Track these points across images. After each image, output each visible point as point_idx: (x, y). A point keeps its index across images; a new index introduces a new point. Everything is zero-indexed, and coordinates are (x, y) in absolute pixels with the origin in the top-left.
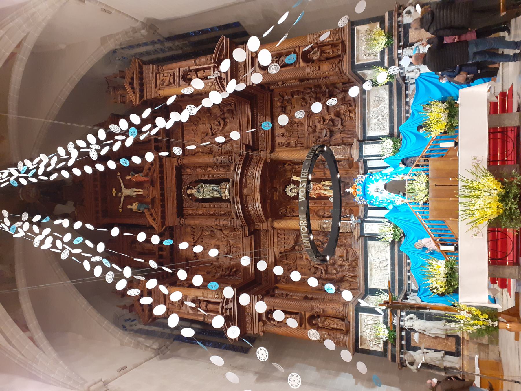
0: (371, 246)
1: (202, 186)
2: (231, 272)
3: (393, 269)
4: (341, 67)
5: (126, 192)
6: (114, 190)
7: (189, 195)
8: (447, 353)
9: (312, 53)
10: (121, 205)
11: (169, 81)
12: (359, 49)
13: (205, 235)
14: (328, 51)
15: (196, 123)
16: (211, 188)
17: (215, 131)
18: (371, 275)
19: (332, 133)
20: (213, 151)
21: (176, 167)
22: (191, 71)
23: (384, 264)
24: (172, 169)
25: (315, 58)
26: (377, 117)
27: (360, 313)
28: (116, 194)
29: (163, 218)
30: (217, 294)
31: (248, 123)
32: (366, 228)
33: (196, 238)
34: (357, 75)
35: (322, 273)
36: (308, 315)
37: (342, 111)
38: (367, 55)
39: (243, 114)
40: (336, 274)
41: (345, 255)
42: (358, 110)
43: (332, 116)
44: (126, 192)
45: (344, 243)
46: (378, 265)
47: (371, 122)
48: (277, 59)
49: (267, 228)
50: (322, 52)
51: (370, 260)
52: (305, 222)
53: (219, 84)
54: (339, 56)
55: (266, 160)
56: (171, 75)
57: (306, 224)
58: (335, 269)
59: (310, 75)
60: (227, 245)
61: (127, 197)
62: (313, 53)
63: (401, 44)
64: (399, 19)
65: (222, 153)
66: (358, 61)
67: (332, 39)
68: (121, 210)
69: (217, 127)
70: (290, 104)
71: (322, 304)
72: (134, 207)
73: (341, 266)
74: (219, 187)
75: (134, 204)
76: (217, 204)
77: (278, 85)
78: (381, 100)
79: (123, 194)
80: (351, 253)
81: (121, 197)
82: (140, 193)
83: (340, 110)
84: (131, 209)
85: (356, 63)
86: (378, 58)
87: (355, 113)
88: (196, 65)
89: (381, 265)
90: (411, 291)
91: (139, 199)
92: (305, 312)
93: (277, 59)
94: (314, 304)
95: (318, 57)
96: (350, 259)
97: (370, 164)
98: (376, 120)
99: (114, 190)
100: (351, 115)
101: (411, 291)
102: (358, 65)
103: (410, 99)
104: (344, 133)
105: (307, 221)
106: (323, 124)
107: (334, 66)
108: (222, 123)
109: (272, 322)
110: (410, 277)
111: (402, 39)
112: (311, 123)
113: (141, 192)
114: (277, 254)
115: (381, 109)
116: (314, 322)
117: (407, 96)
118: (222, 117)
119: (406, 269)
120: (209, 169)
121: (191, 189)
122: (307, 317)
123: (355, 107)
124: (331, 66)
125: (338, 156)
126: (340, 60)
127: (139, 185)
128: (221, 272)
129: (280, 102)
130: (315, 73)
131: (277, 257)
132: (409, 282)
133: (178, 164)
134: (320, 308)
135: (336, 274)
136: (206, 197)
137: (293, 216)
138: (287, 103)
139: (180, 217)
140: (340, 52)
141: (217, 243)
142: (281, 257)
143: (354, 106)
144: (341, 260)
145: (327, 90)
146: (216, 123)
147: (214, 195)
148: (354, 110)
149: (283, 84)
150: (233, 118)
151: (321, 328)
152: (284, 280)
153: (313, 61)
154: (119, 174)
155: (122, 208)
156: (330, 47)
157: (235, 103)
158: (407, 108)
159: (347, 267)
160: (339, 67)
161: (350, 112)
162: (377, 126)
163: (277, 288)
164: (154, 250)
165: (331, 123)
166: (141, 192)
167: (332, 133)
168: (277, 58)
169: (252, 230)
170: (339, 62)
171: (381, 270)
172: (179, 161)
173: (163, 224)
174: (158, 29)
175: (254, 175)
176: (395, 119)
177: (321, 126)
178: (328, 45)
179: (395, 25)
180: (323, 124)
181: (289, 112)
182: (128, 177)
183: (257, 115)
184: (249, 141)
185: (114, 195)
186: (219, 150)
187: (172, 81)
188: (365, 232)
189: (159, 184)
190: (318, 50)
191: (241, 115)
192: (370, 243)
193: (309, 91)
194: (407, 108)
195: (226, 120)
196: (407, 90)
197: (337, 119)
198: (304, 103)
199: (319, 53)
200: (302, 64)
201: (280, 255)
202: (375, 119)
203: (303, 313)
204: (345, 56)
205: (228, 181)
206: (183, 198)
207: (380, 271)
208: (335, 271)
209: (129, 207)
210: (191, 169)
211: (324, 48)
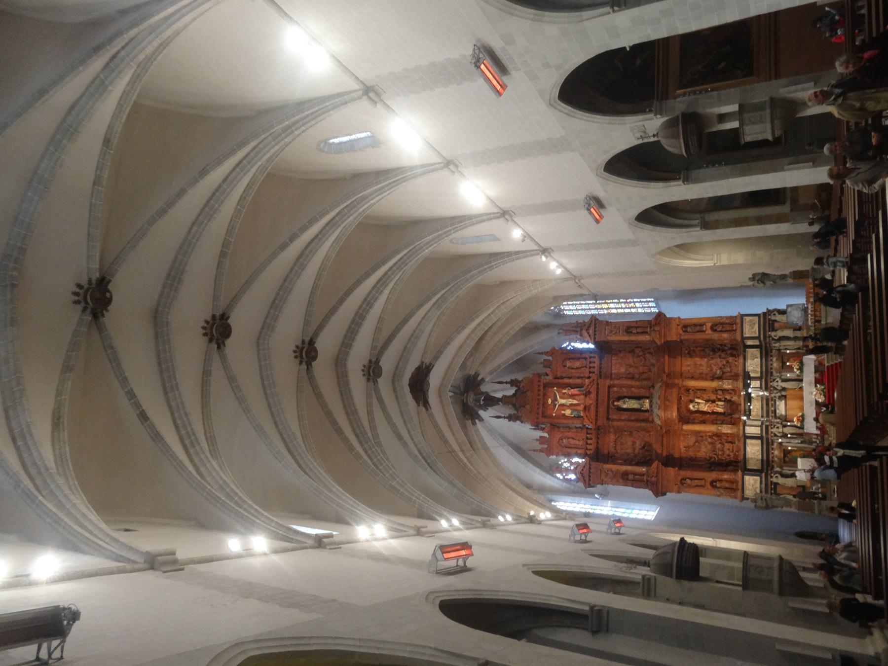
5: (563, 401)
7: (614, 405)
23: (758, 453)
25: (718, 330)
36: (710, 480)
44: (563, 401)
54: (734, 330)
61: (563, 405)
72: (568, 412)
76: (637, 413)
86: (757, 335)
100: (736, 363)
151: (719, 488)
158: (771, 363)
167: (724, 373)
179: (767, 320)
192: (748, 441)
194: (771, 363)
205: (648, 398)
209: (563, 412)
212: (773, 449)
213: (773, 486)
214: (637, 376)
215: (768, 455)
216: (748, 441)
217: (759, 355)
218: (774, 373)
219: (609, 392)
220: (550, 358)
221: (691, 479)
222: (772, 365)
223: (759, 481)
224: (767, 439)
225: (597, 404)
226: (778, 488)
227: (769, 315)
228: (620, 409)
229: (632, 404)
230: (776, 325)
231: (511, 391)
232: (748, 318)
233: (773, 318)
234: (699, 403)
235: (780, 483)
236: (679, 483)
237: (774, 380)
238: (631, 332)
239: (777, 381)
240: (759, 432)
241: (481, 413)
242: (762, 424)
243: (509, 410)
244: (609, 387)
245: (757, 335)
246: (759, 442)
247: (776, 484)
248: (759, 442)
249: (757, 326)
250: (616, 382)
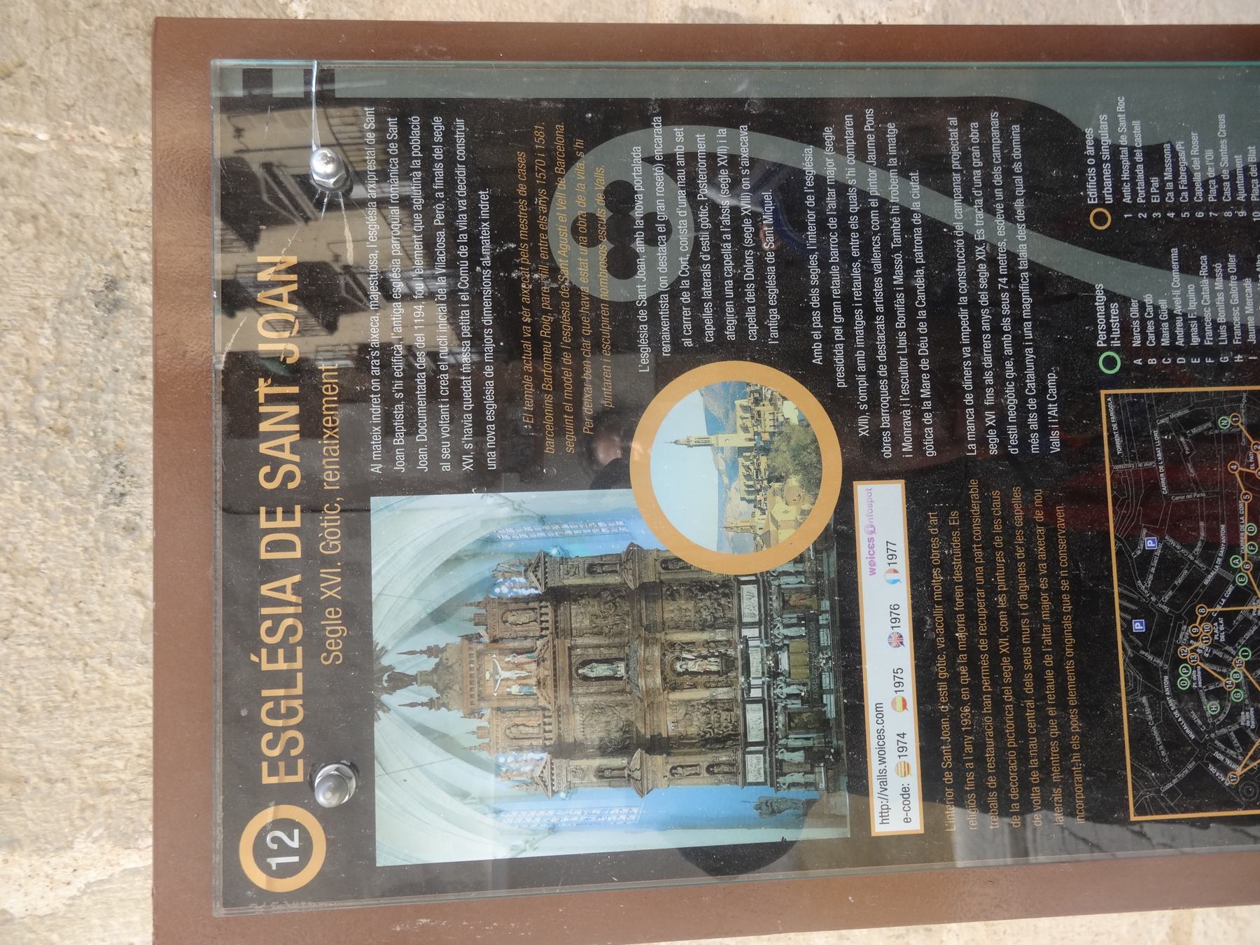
7: (578, 675)
8: (806, 773)
36: (705, 765)
61: (507, 679)
72: (515, 689)
73: (726, 727)
192: (748, 706)
205: (621, 660)
209: (508, 690)
212: (776, 714)
214: (606, 630)
215: (771, 724)
216: (748, 706)
218: (775, 616)
219: (570, 656)
220: (483, 611)
224: (770, 702)
225: (555, 675)
228: (586, 678)
229: (602, 670)
231: (429, 664)
236: (668, 774)
237: (775, 626)
241: (385, 698)
243: (430, 692)
244: (570, 649)
246: (761, 706)
248: (761, 706)
250: (579, 641)
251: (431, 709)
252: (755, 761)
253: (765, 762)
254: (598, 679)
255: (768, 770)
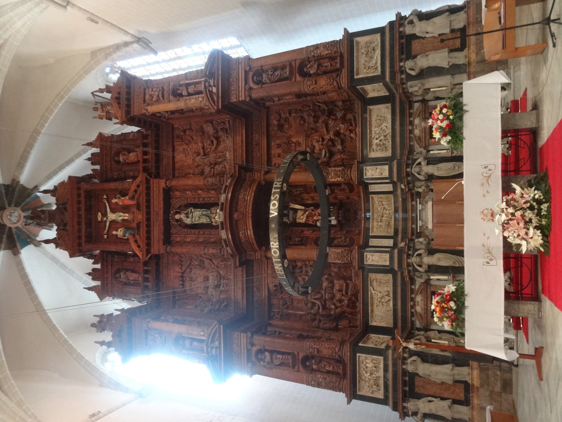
0: (372, 279)
1: (191, 210)
2: (220, 306)
3: (395, 305)
4: (339, 82)
5: (112, 216)
6: (100, 214)
7: (177, 221)
9: (308, 66)
10: (106, 231)
11: (158, 96)
12: (358, 62)
13: (193, 265)
14: (326, 64)
15: (187, 142)
16: (200, 213)
17: (207, 151)
18: (372, 311)
19: (332, 154)
20: (204, 172)
21: (164, 189)
22: (181, 85)
23: (387, 298)
24: (159, 191)
25: (312, 72)
26: (379, 137)
27: (358, 354)
28: (101, 219)
29: (149, 244)
30: (203, 331)
31: (242, 141)
32: (367, 259)
33: (184, 268)
34: (357, 91)
35: (319, 308)
37: (342, 131)
38: (367, 68)
39: (237, 133)
40: (334, 309)
41: (344, 289)
42: (358, 130)
43: (331, 136)
44: (112, 216)
45: (344, 275)
46: (379, 300)
47: (373, 143)
48: (272, 73)
49: (259, 258)
50: (319, 65)
51: (371, 294)
52: (277, 243)
53: (210, 99)
55: (259, 182)
56: (160, 90)
57: (278, 247)
58: (334, 304)
59: (306, 90)
60: (217, 276)
61: (113, 222)
62: (310, 67)
63: (404, 56)
64: (401, 29)
65: (214, 175)
66: (357, 75)
67: (330, 52)
68: (106, 236)
69: (210, 147)
70: (288, 123)
71: (317, 343)
72: (120, 233)
73: (340, 301)
74: (209, 212)
75: (119, 230)
76: (207, 231)
77: (274, 102)
78: (382, 119)
79: (109, 219)
80: (350, 286)
81: (106, 222)
82: (126, 218)
83: (340, 129)
84: (117, 235)
85: (355, 77)
86: (379, 72)
87: (356, 133)
88: (187, 80)
89: (383, 300)
90: (415, 329)
91: (125, 224)
92: (298, 353)
93: (272, 73)
94: (308, 343)
95: (315, 71)
96: (349, 293)
97: (373, 188)
98: (377, 141)
99: (100, 214)
100: (352, 135)
101: (415, 329)
102: (357, 79)
103: (414, 119)
104: (344, 155)
105: (279, 242)
106: (322, 145)
107: (332, 80)
108: (215, 142)
109: (262, 363)
110: (415, 313)
111: (405, 51)
112: (310, 143)
113: (126, 216)
114: (271, 286)
115: (383, 129)
116: (307, 363)
117: (411, 115)
118: (215, 135)
119: (409, 305)
120: (200, 192)
121: (180, 213)
122: (301, 357)
123: (356, 126)
124: (329, 81)
125: (337, 179)
126: (338, 74)
127: (125, 209)
128: (210, 306)
129: (277, 121)
130: (311, 87)
131: (272, 291)
132: (413, 319)
133: (167, 186)
134: (314, 348)
135: (334, 309)
136: (195, 223)
137: (290, 245)
138: (285, 121)
139: (167, 245)
140: (338, 66)
141: (206, 274)
142: (275, 290)
143: (354, 126)
144: (340, 294)
145: (326, 108)
146: (209, 142)
147: (204, 220)
148: (355, 130)
149: (279, 100)
150: (227, 137)
152: (279, 316)
153: (310, 75)
154: (105, 197)
155: (107, 234)
156: (328, 60)
157: (229, 122)
158: (410, 128)
159: (346, 302)
160: (337, 82)
161: (351, 131)
162: (379, 147)
163: (270, 325)
164: (139, 281)
165: (330, 143)
166: (126, 216)
167: (332, 154)
168: (272, 71)
169: (244, 260)
170: (337, 76)
171: (383, 305)
172: (167, 182)
173: (148, 252)
174: (151, 43)
175: (246, 199)
176: (398, 139)
177: (320, 146)
178: (326, 58)
180: (322, 145)
181: (287, 131)
182: (114, 201)
183: (252, 133)
184: (243, 161)
185: (99, 219)
186: (211, 171)
187: (160, 96)
188: (365, 263)
189: (145, 207)
190: (315, 63)
191: (235, 134)
192: (372, 276)
193: (307, 109)
194: (410, 128)
195: (219, 139)
196: (411, 109)
197: (337, 139)
198: (302, 122)
199: (316, 66)
200: (298, 78)
201: (274, 288)
202: (377, 139)
203: (296, 353)
204: (343, 70)
206: (171, 224)
207: (381, 306)
208: (333, 307)
209: (114, 233)
210: (180, 192)
211: (322, 61)
212: (412, 291)
213: (407, 378)
214: (207, 170)
217: (389, 117)
221: (272, 352)
222: (411, 132)
223: (382, 366)
226: (418, 382)
227: (401, 25)
230: (416, 45)
232: (362, 40)
233: (408, 30)
234: (296, 210)
235: (421, 372)
238: (181, 95)
239: (419, 164)
240: (388, 263)
242: (395, 245)
245: (379, 72)
246: (390, 277)
247: (413, 376)
248: (390, 277)
249: (378, 52)
251: (56, 247)
252: (370, 365)
253: (386, 370)
254: (194, 226)
255: (390, 383)
